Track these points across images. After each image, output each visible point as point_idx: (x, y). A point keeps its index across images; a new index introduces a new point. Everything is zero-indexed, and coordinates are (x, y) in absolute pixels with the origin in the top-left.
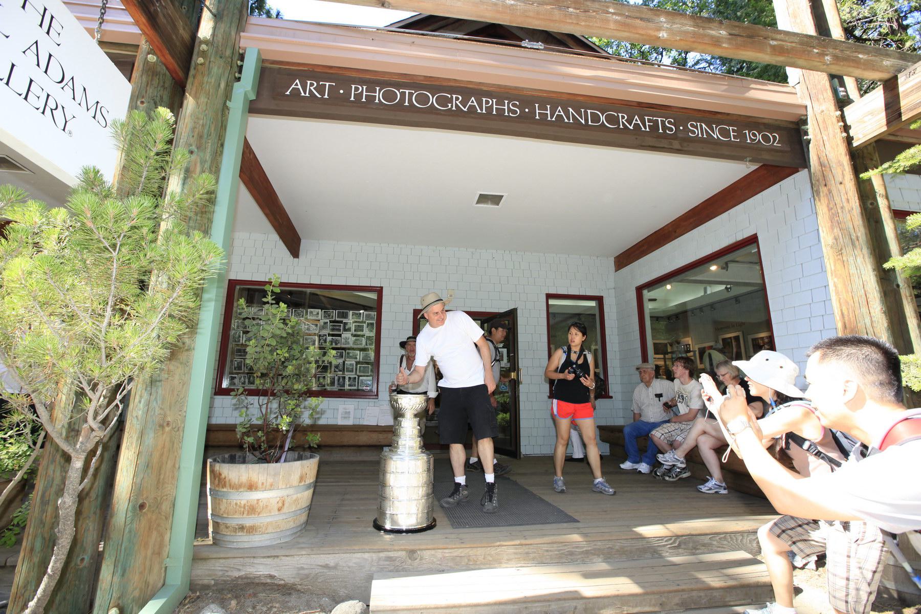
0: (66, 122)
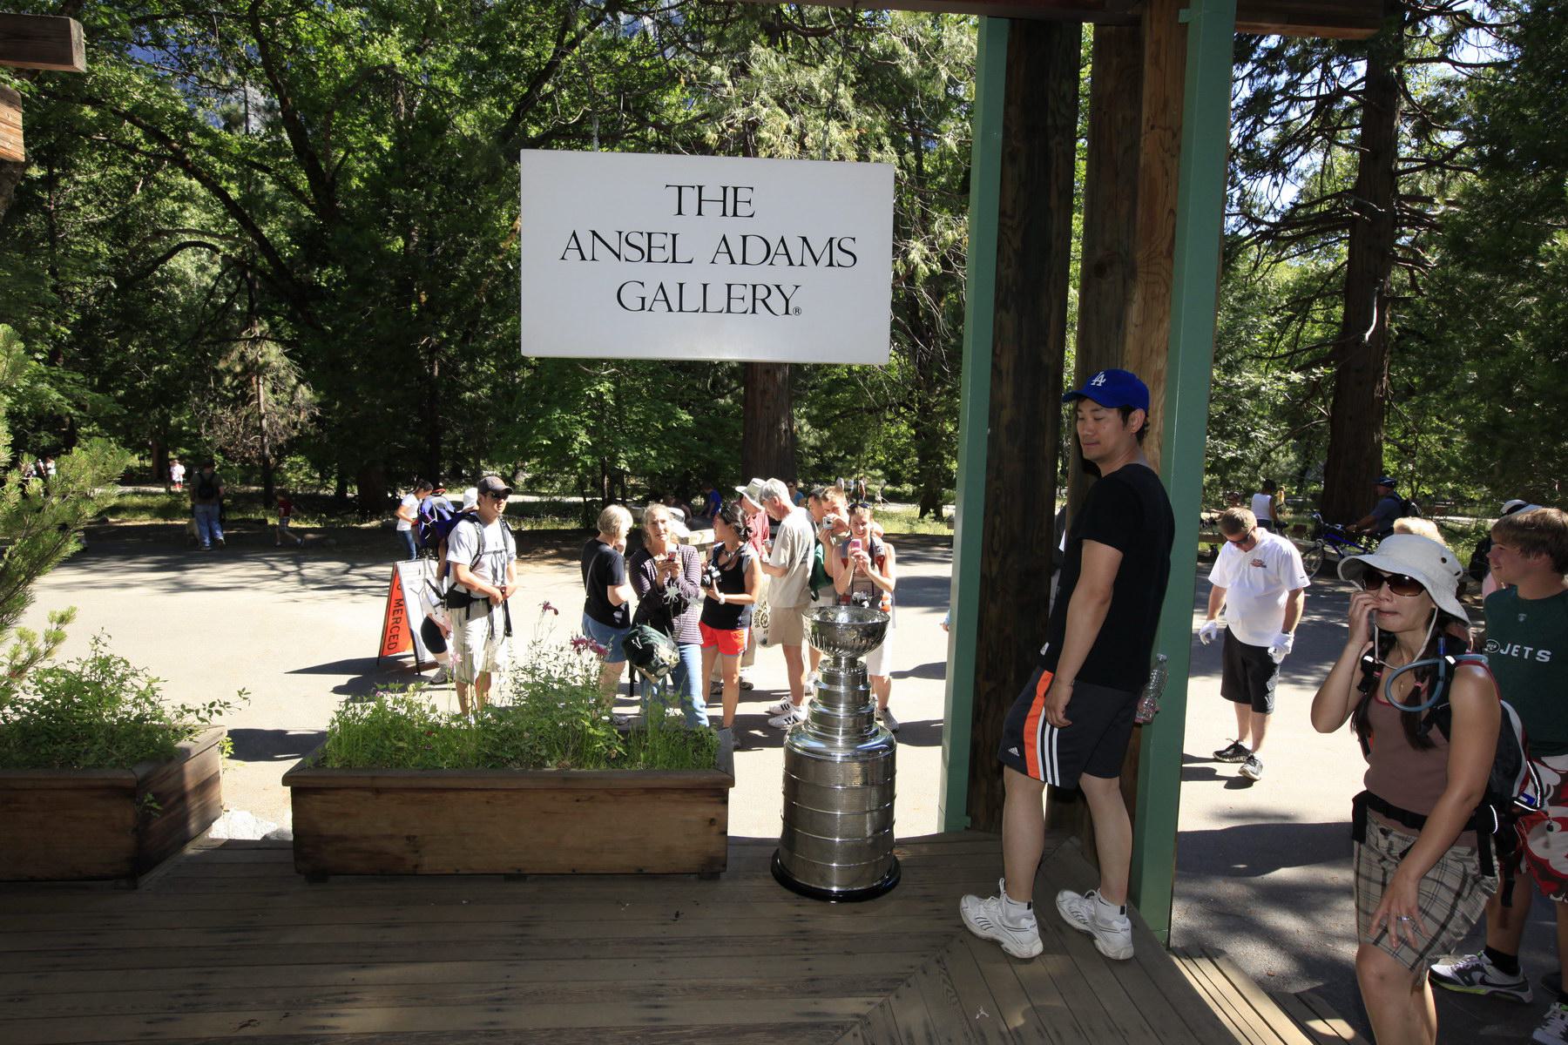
0: (787, 301)
